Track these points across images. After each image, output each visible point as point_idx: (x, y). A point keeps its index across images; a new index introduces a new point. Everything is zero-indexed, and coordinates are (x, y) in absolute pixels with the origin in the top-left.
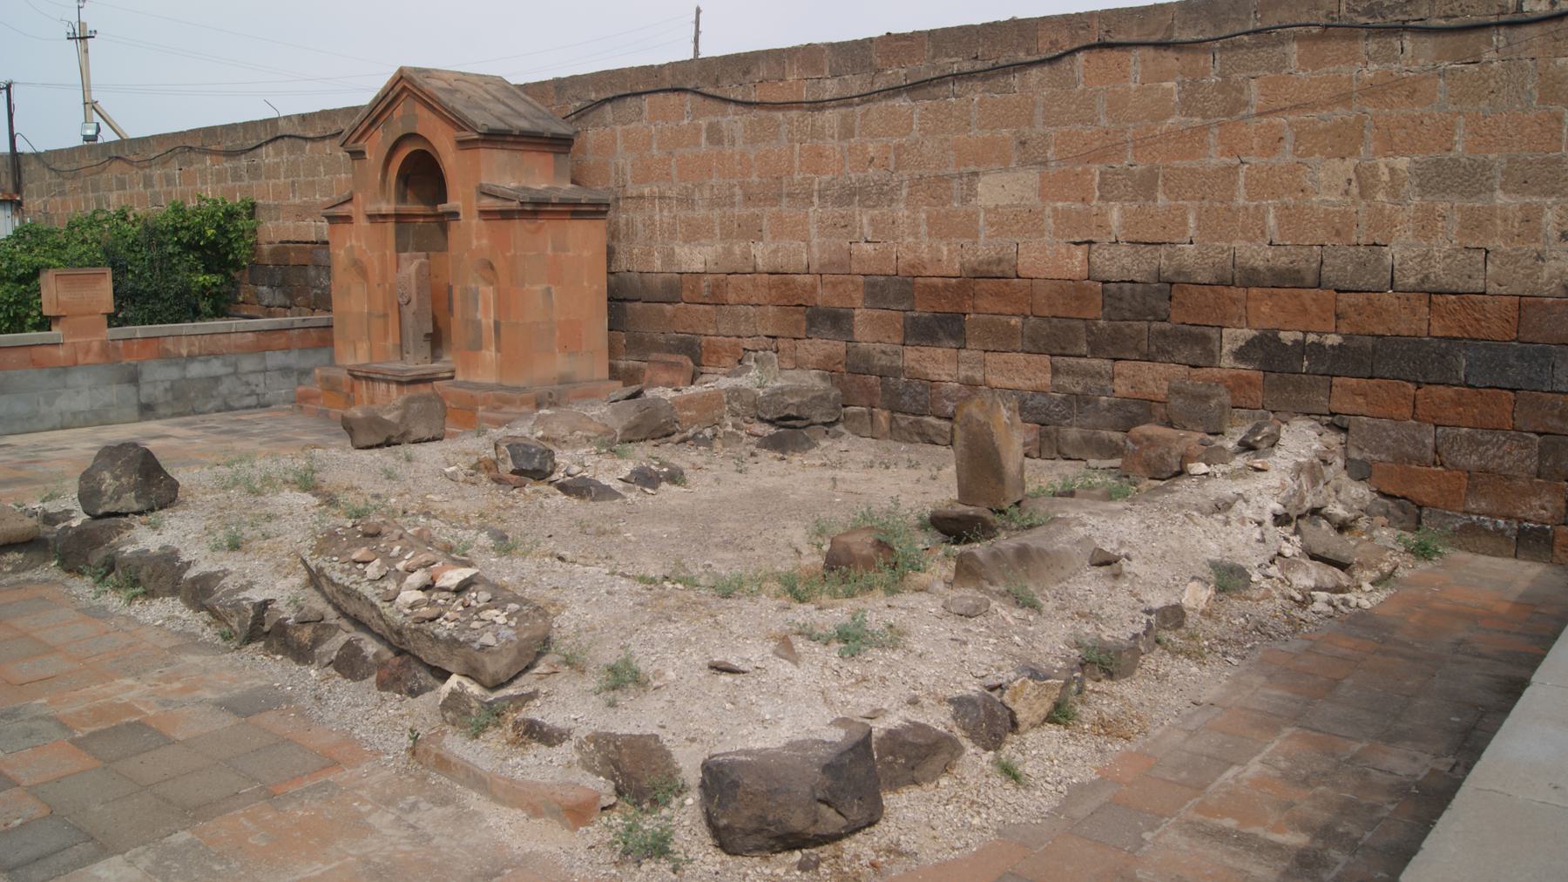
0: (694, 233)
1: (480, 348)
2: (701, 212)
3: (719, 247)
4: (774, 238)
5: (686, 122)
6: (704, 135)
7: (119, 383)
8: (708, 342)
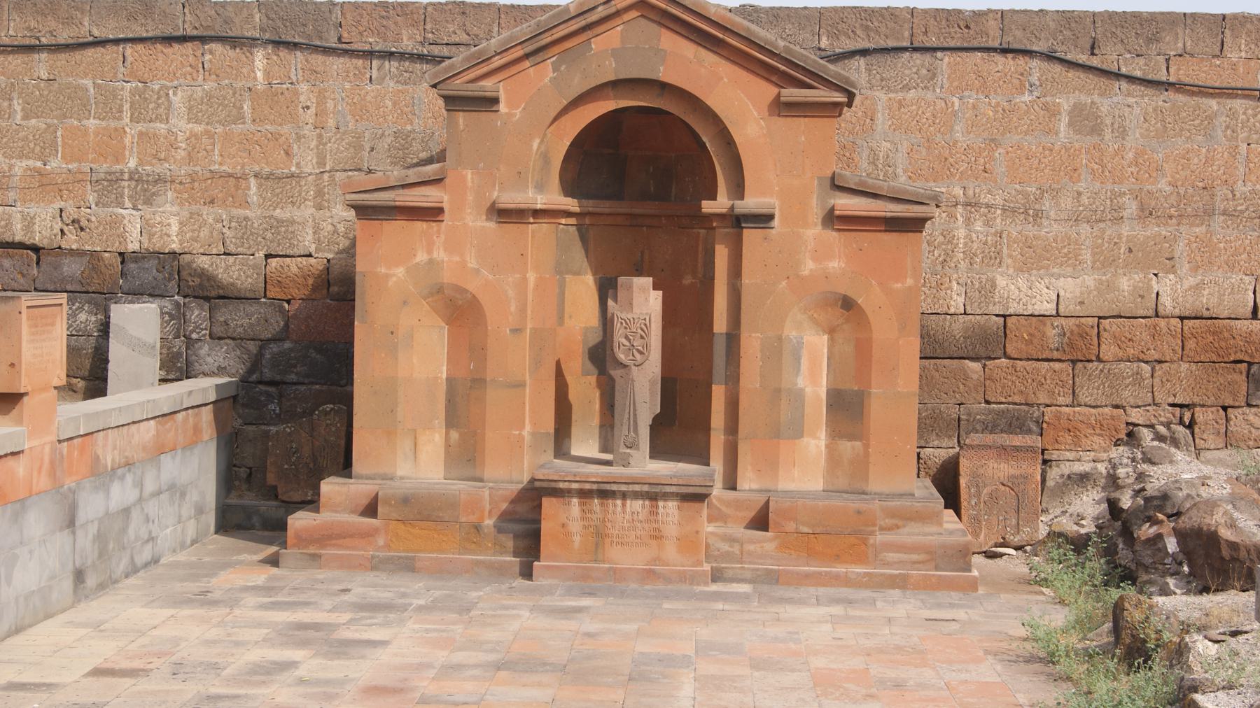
0: (1035, 259)
1: (799, 434)
2: (1052, 229)
3: (1090, 280)
4: (1195, 269)
5: (1027, 98)
6: (1065, 120)
7: (61, 529)
8: (1058, 417)
